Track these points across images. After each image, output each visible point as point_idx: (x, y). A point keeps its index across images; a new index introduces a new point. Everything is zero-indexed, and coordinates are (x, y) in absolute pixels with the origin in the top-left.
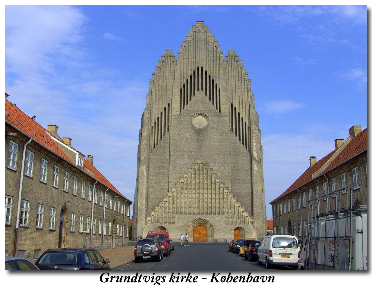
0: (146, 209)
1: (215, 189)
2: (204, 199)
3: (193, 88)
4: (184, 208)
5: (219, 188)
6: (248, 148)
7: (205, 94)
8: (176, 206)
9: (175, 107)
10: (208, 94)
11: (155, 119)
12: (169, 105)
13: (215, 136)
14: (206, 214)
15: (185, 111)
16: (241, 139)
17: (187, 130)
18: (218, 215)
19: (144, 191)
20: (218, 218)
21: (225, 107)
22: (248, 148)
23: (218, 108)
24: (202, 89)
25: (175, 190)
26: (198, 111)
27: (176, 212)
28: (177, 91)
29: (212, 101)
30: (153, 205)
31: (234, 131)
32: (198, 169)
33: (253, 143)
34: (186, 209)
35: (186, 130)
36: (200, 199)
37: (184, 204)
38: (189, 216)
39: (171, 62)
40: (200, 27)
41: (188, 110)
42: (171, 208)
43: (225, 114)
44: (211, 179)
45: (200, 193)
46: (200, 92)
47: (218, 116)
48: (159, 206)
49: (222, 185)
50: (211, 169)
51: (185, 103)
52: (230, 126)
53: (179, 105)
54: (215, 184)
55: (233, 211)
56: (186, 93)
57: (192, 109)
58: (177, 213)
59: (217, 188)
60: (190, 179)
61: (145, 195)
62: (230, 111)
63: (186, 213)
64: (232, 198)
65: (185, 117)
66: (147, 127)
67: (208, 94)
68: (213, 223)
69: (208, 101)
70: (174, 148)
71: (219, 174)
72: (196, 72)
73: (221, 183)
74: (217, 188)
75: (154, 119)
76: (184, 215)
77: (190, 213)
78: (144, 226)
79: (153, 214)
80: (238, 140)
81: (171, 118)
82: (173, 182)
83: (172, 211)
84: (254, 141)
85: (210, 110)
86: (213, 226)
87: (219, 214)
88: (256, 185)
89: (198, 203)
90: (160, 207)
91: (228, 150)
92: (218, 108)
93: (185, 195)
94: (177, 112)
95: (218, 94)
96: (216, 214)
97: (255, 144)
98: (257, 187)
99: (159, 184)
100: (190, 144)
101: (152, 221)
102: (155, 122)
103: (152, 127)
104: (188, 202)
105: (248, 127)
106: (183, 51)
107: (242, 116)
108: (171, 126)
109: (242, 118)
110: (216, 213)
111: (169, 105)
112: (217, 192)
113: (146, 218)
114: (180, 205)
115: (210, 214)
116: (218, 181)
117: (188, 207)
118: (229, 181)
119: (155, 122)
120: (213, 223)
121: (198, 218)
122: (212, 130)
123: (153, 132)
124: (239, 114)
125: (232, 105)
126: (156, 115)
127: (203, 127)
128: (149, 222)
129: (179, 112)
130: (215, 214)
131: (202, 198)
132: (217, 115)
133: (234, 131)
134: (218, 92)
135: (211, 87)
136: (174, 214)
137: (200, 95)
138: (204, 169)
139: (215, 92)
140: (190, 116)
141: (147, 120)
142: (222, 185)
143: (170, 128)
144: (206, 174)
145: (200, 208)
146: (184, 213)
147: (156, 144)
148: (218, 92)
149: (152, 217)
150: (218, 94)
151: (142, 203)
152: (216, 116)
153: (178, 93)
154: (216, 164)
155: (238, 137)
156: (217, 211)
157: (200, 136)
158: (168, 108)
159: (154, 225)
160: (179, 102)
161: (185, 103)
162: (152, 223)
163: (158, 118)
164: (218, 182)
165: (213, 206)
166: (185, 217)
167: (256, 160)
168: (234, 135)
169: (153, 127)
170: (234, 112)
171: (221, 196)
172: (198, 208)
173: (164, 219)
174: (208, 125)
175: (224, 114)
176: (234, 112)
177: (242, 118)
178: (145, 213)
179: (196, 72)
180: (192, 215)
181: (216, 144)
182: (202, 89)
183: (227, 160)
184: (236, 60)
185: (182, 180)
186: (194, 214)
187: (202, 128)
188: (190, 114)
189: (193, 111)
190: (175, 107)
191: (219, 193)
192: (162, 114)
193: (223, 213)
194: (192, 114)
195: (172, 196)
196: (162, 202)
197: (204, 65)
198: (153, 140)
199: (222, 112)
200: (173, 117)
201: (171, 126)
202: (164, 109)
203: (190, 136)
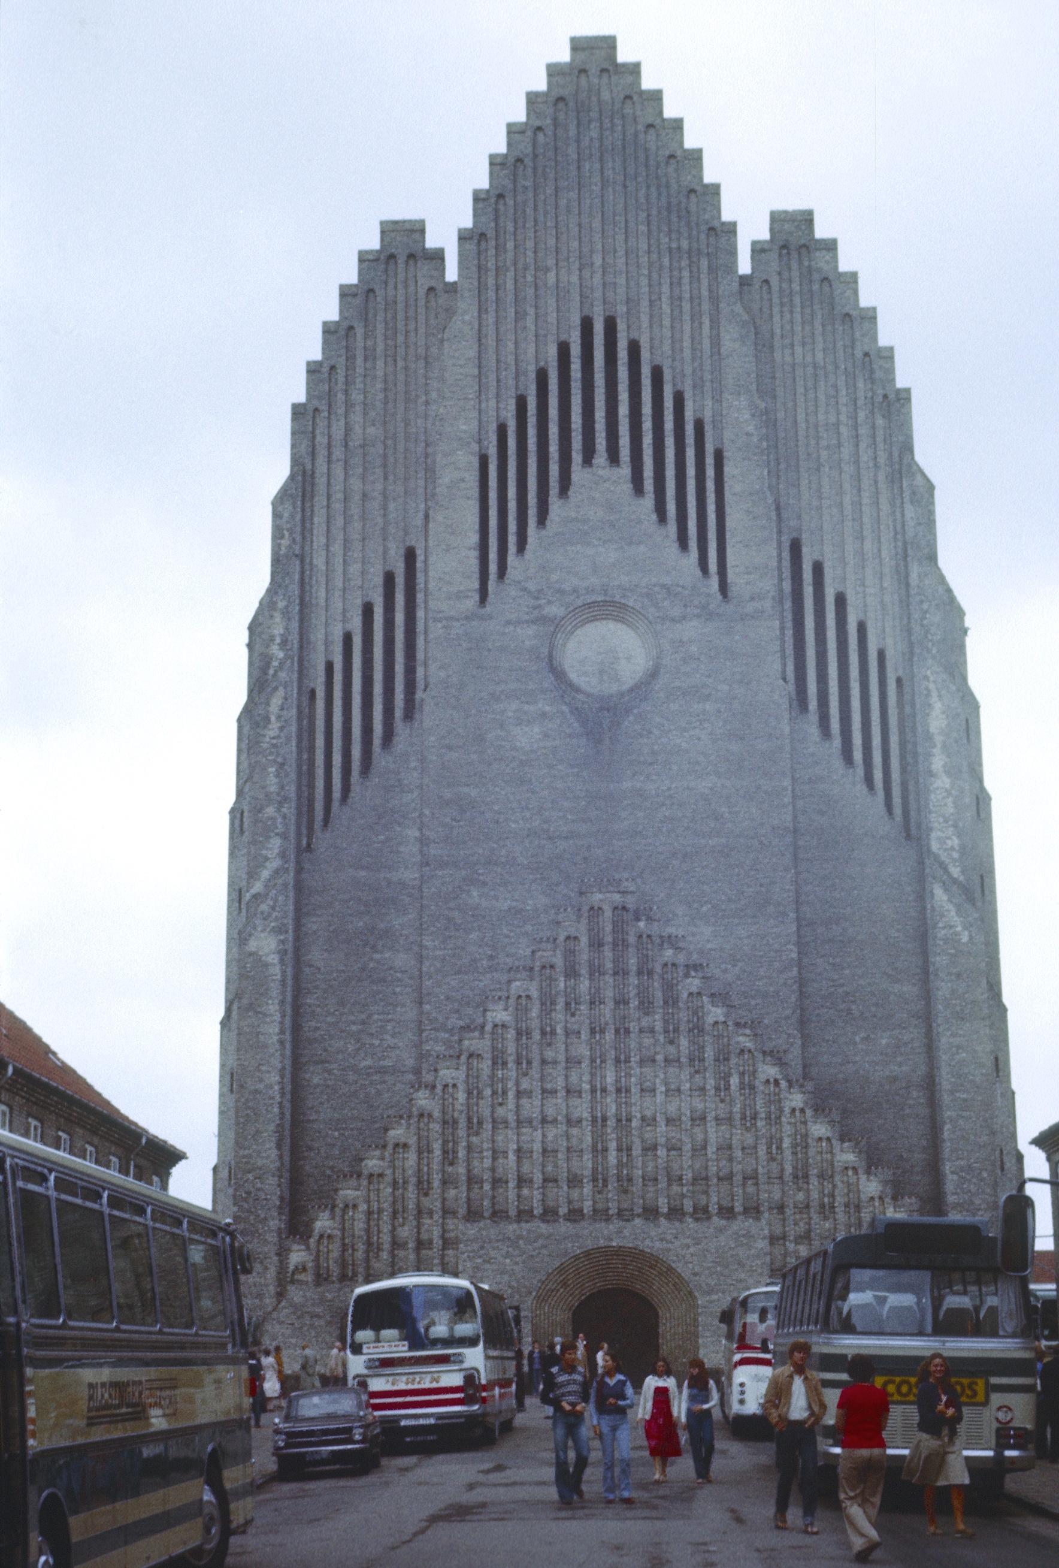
0: (282, 1198)
2: (635, 1123)
3: (554, 449)
4: (511, 1185)
5: (723, 1057)
6: (898, 810)
7: (628, 487)
8: (462, 1170)
9: (450, 564)
10: (649, 485)
11: (327, 643)
12: (410, 556)
13: (699, 739)
14: (651, 1213)
15: (513, 593)
16: (858, 755)
17: (526, 707)
18: (723, 1222)
19: (271, 1087)
20: (722, 1238)
21: (752, 557)
22: (898, 810)
23: (713, 566)
24: (614, 458)
25: (454, 1073)
26: (589, 591)
27: (462, 1211)
28: (458, 471)
29: (672, 527)
30: (328, 1172)
31: (813, 705)
32: (596, 944)
33: (931, 774)
34: (525, 1192)
35: (515, 705)
36: (611, 1123)
37: (512, 1157)
38: (544, 1228)
39: (422, 292)
40: (593, 70)
41: (532, 586)
42: (436, 1183)
43: (756, 604)
45: (611, 1088)
46: (601, 472)
47: (711, 616)
48: (359, 1176)
49: (744, 1040)
51: (512, 539)
52: (784, 679)
53: (474, 554)
54: (697, 1029)
55: (815, 1195)
56: (519, 486)
57: (554, 577)
58: (473, 1215)
59: (709, 1053)
60: (547, 1003)
61: (276, 1110)
62: (787, 586)
63: (524, 1215)
64: (809, 1113)
65: (511, 628)
66: (281, 692)
67: (649, 485)
68: (695, 1274)
70: (448, 820)
71: (725, 971)
72: (575, 350)
73: (737, 1024)
74: (709, 1053)
75: (321, 648)
76: (515, 1226)
77: (549, 1214)
78: (269, 1301)
79: (323, 1223)
80: (838, 763)
81: (426, 632)
82: (443, 1028)
83: (438, 1204)
84: (938, 763)
85: (667, 580)
86: (691, 1293)
87: (727, 1212)
88: (953, 1035)
89: (599, 1150)
90: (365, 1183)
91: (776, 822)
92: (713, 566)
93: (518, 1106)
94: (459, 596)
95: (710, 485)
96: (709, 1218)
97: (943, 782)
98: (958, 1047)
99: (358, 1041)
100: (546, 792)
101: (318, 1267)
102: (329, 667)
103: (313, 693)
104: (537, 1147)
105: (899, 681)
106: (493, 224)
107: (861, 616)
108: (426, 687)
109: (862, 628)
110: (713, 1209)
111: (410, 556)
112: (711, 1083)
113: (283, 1253)
114: (487, 1163)
115: (676, 1213)
116: (715, 1013)
117: (538, 1177)
118: (788, 1012)
119: (329, 667)
120: (695, 1274)
121: (602, 1243)
122: (675, 707)
123: (320, 723)
124: (841, 600)
125: (796, 547)
126: (336, 619)
127: (626, 687)
128: (302, 1277)
129: (477, 597)
130: (701, 1213)
131: (623, 1122)
133: (813, 705)
134: (710, 472)
135: (670, 442)
136: (451, 1223)
137: (600, 488)
138: (632, 939)
139: (691, 471)
140: (543, 620)
141: (281, 655)
142: (744, 1040)
143: (419, 695)
145: (612, 1185)
146: (512, 1213)
147: (337, 794)
148: (710, 472)
149: (319, 1242)
150: (710, 485)
151: (260, 1163)
152: (698, 616)
153: (463, 480)
154: (704, 909)
155: (837, 742)
156: (714, 1199)
157: (607, 742)
158: (404, 582)
159: (329, 1296)
160: (474, 538)
161: (512, 539)
162: (321, 1278)
163: (348, 639)
164: (722, 1019)
166: (520, 1237)
167: (949, 883)
168: (814, 731)
169: (320, 694)
170: (808, 590)
171: (737, 1109)
172: (599, 1179)
173: (393, 1256)
174: (653, 674)
175: (750, 608)
176: (808, 590)
177: (862, 628)
178: (275, 1223)
179: (575, 350)
180: (564, 1228)
182: (614, 458)
183: (774, 883)
184: (819, 270)
185: (500, 1014)
186: (575, 1215)
187: (614, 688)
188: (539, 607)
189: (561, 591)
190: (450, 564)
192: (368, 610)
193: (753, 1210)
194: (554, 610)
195: (436, 1114)
196: (377, 1153)
197: (621, 309)
198: (320, 772)
199: (733, 590)
200: (437, 630)
201: (426, 687)
202: (379, 580)
203: (541, 744)
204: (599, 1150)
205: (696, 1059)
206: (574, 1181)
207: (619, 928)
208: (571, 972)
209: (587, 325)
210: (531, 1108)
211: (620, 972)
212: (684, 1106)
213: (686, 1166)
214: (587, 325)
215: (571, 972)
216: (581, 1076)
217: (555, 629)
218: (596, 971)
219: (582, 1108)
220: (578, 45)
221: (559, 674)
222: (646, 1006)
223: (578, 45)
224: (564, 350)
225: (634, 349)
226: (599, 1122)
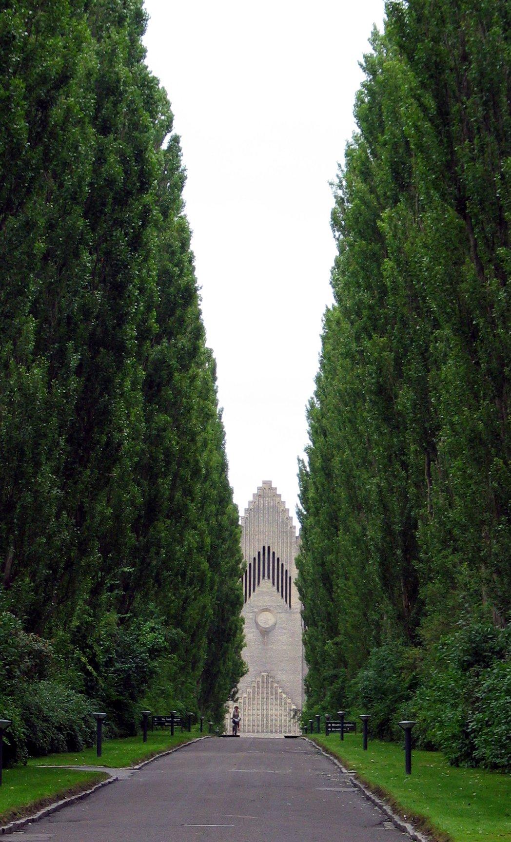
1: (281, 705)
5: (285, 704)
24: (269, 577)
32: (263, 682)
44: (276, 694)
49: (289, 701)
50: (278, 682)
60: (254, 693)
69: (276, 593)
89: (263, 720)
116: (284, 696)
131: (267, 715)
132: (286, 612)
144: (272, 687)
165: (278, 723)
172: (262, 726)
181: (285, 647)
182: (269, 577)
185: (245, 695)
191: (285, 710)
204: (263, 720)
205: (281, 705)
206: (258, 726)
207: (267, 680)
208: (258, 688)
209: (264, 548)
210: (251, 712)
211: (267, 688)
212: (279, 713)
213: (278, 723)
214: (264, 548)
215: (258, 688)
216: (260, 707)
217: (256, 614)
218: (263, 687)
219: (260, 712)
220: (264, 483)
221: (257, 623)
222: (272, 694)
223: (264, 483)
224: (259, 553)
225: (274, 553)
226: (263, 715)
